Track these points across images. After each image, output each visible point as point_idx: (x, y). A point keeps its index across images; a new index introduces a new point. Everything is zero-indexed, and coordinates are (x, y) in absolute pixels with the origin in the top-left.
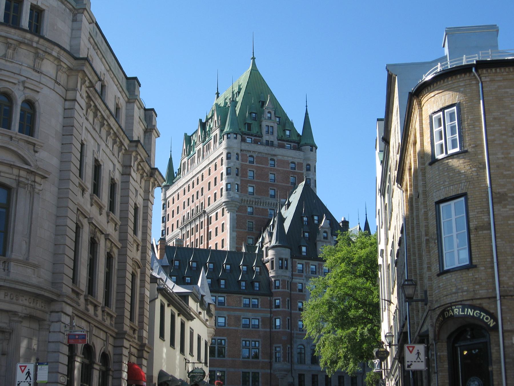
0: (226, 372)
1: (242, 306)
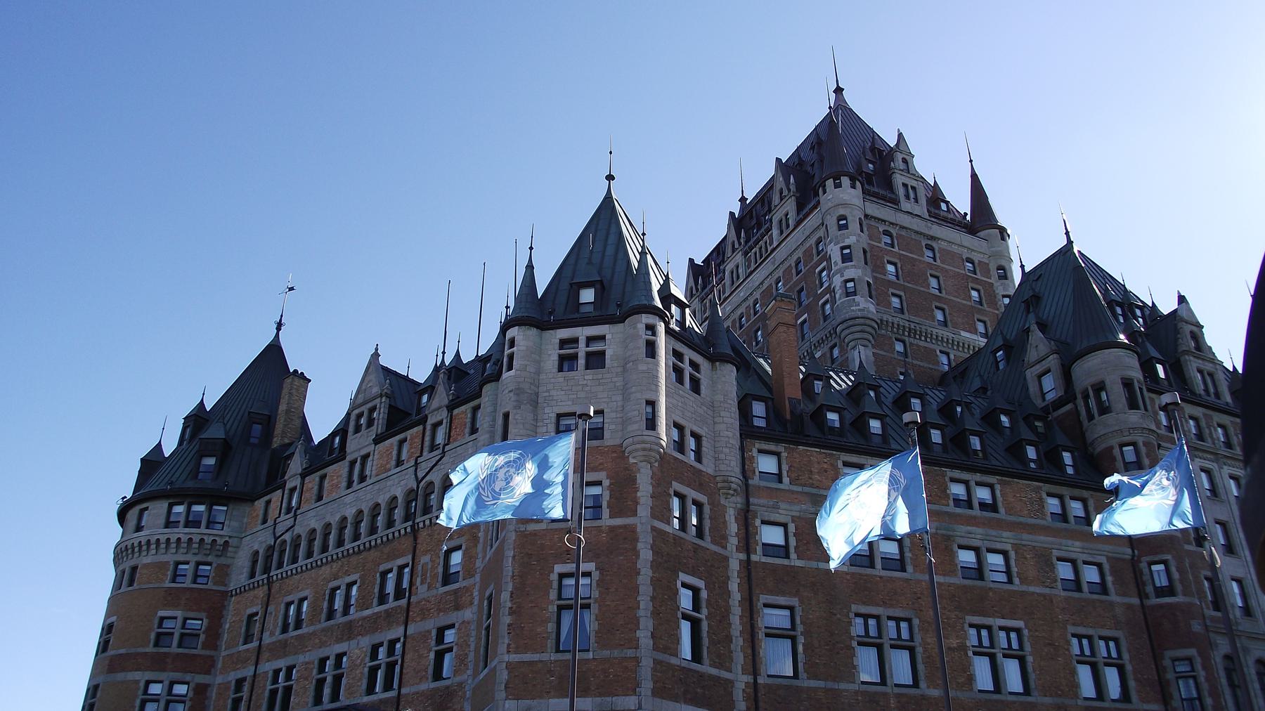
1: (1049, 518)
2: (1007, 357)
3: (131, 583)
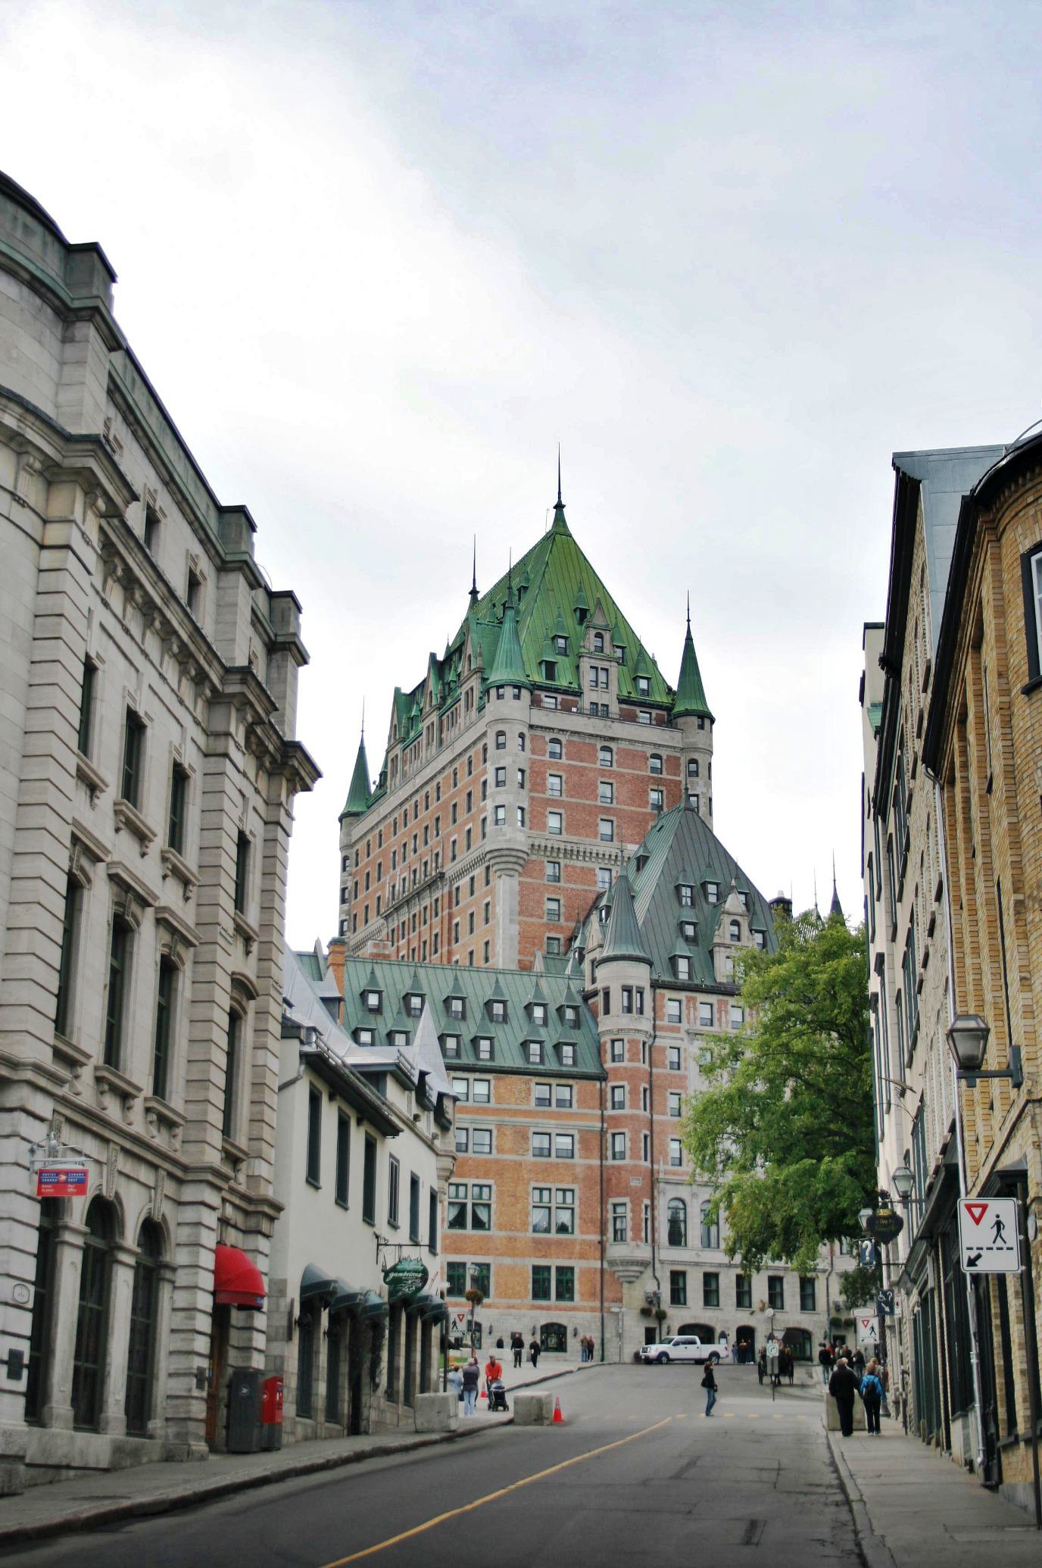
0: (493, 1269)
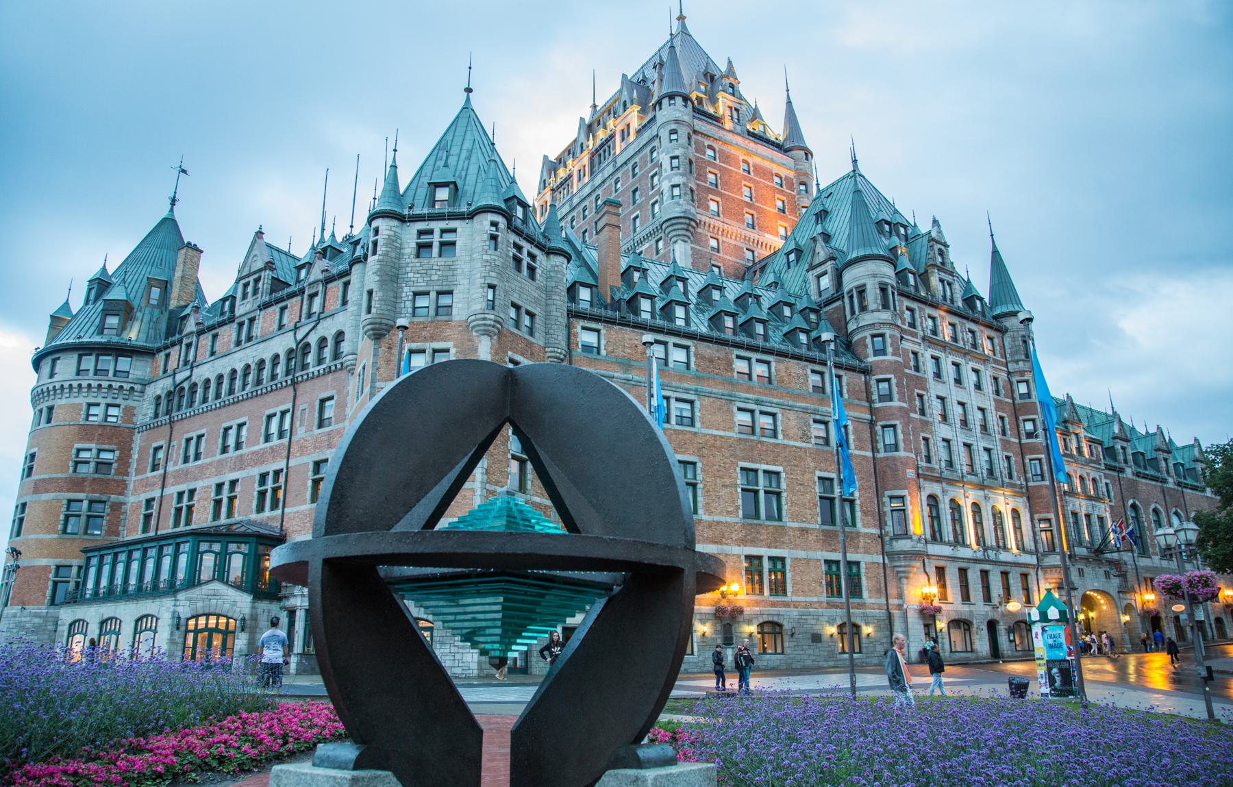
2: (798, 261)
3: (49, 421)
